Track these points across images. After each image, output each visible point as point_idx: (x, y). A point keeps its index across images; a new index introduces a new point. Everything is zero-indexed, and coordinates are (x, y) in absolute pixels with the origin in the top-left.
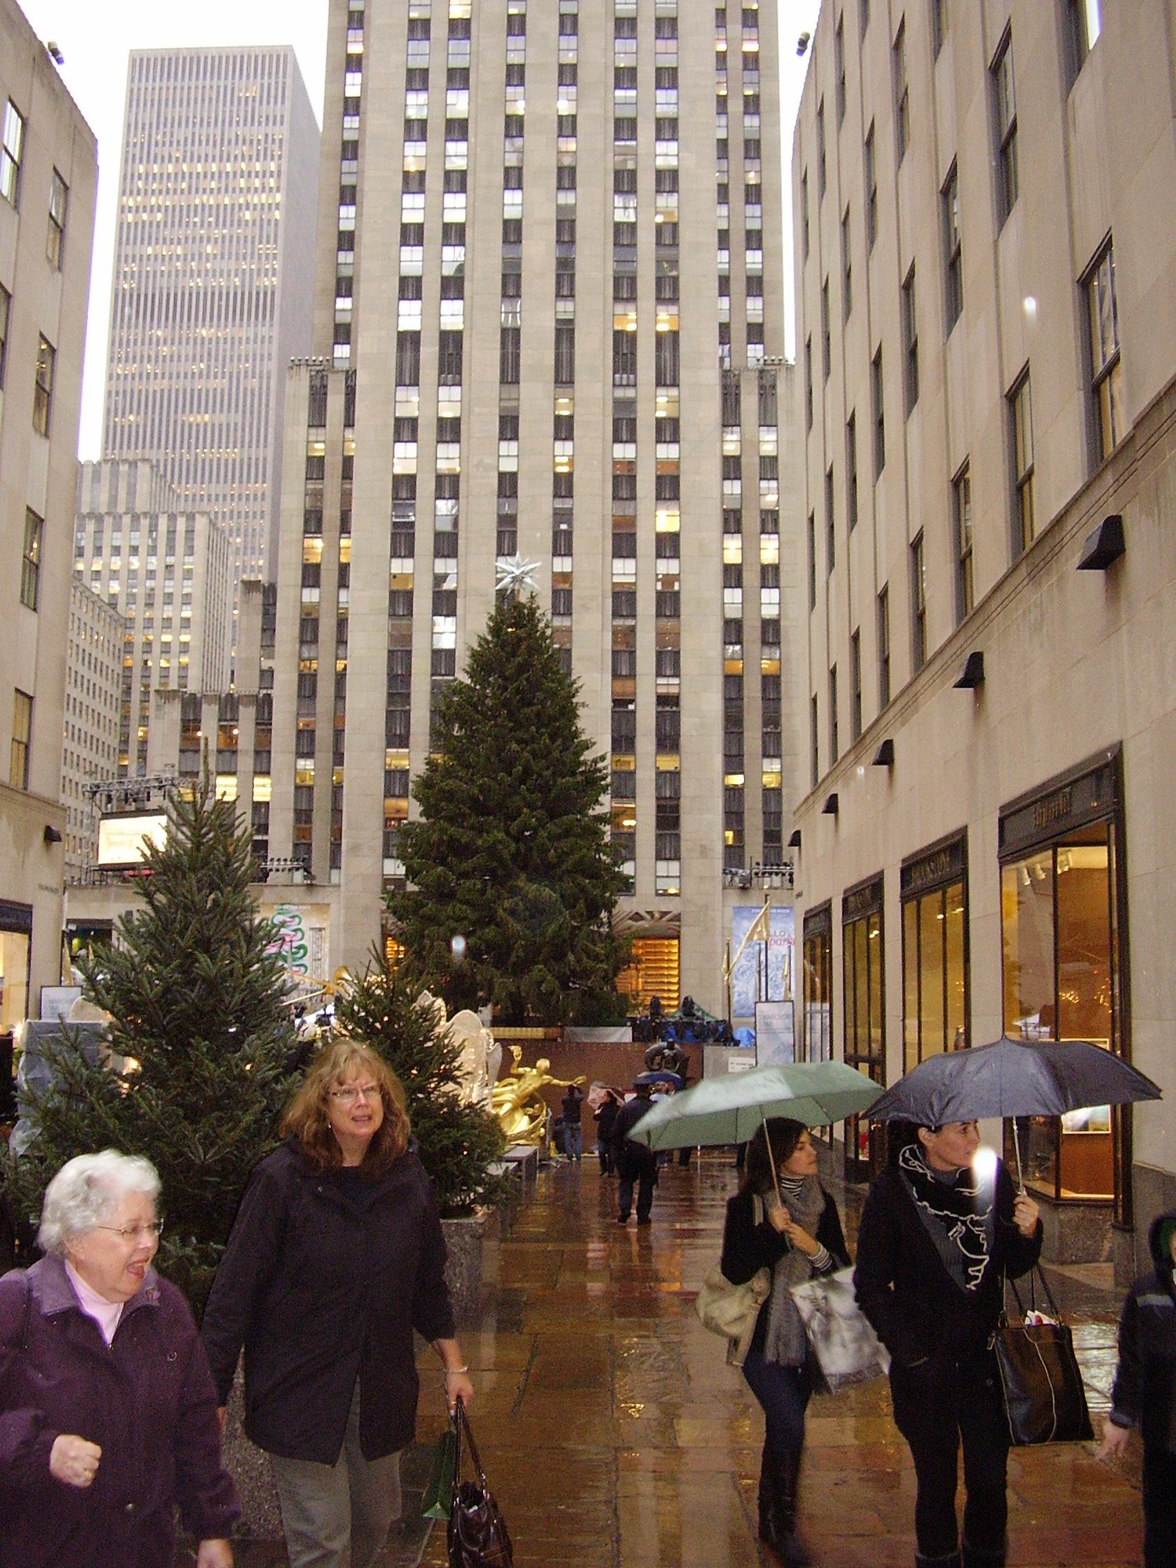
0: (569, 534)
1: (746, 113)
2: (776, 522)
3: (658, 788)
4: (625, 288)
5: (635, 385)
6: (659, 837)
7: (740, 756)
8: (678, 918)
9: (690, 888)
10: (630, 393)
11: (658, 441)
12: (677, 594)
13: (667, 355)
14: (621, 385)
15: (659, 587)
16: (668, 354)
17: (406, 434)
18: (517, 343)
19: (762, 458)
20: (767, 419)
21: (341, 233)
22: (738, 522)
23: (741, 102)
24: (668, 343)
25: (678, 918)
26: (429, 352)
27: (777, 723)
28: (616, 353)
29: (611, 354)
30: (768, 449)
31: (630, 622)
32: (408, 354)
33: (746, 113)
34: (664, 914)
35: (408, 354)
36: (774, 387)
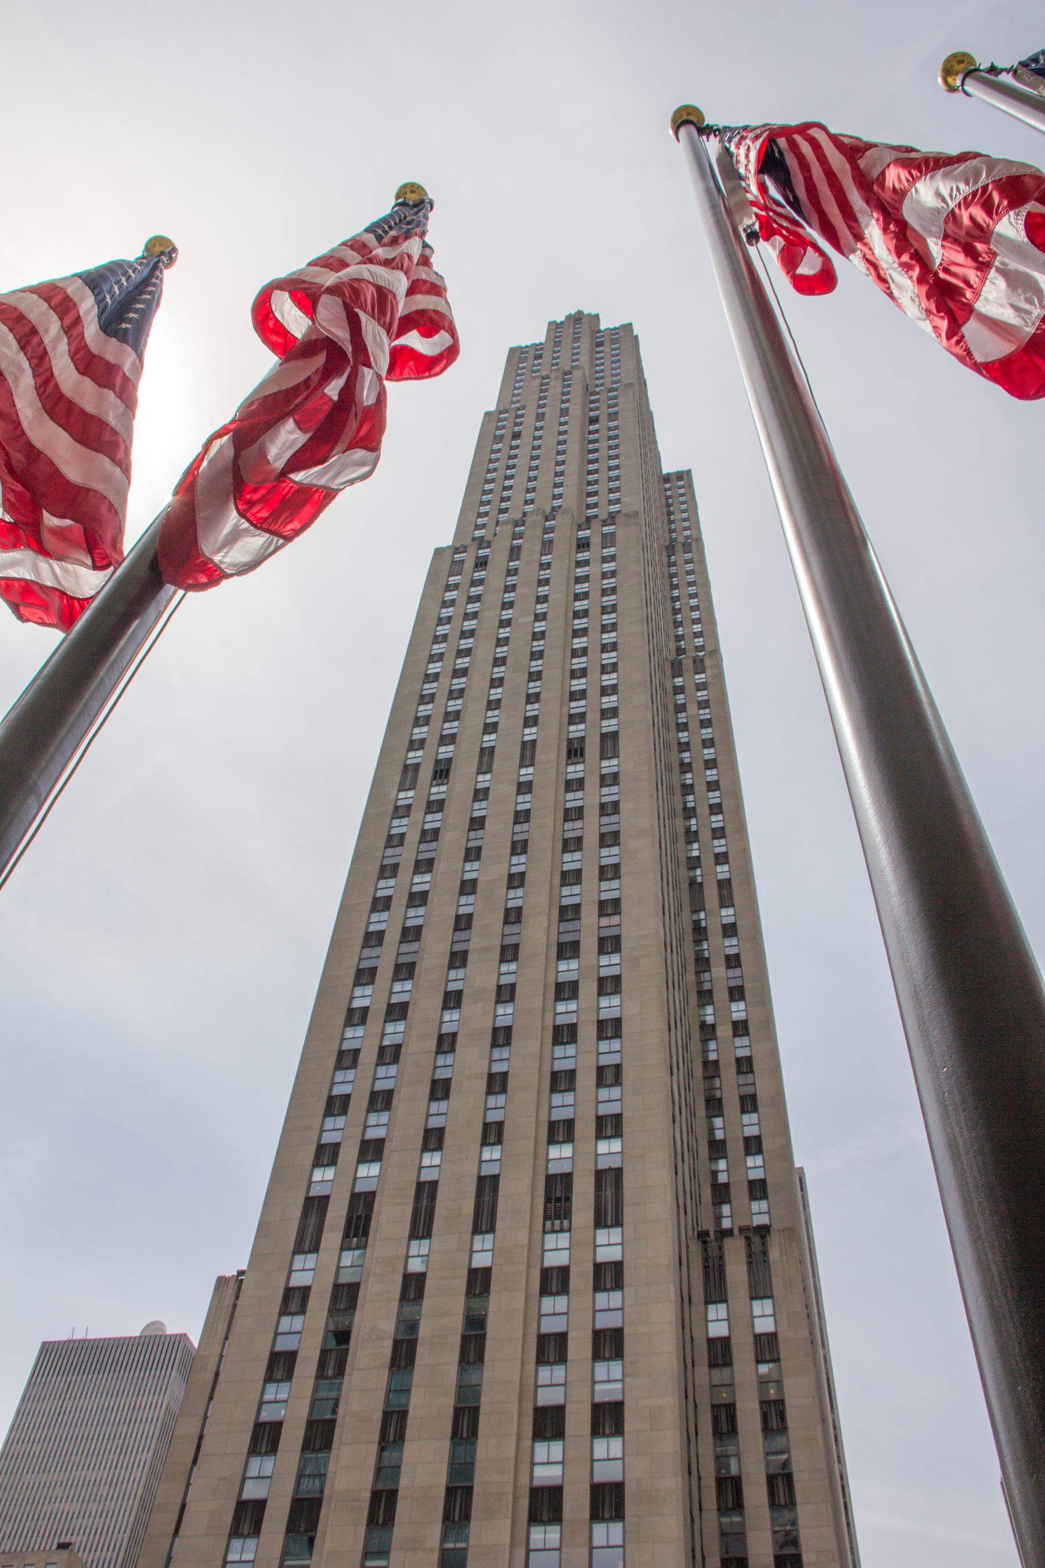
5: (570, 1230)
13: (609, 1193)
14: (553, 1231)
16: (609, 1193)
17: (294, 1306)
18: (433, 1197)
19: (757, 1337)
20: (760, 1290)
23: (730, 1027)
26: (337, 1214)
28: (548, 1200)
29: (540, 1200)
30: (764, 1326)
32: (313, 1220)
35: (313, 1220)
36: (765, 1253)
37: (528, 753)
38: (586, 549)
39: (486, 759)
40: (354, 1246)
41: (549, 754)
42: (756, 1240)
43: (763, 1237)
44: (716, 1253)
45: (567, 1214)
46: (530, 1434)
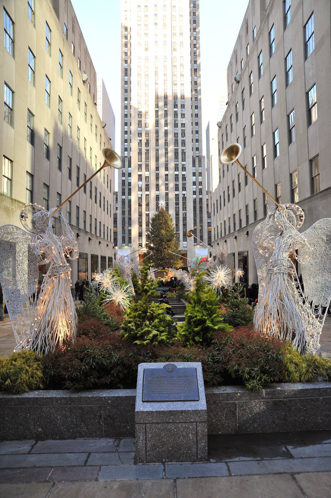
0: (168, 187)
1: (195, 109)
2: (201, 184)
3: (183, 230)
6: (183, 238)
7: (196, 223)
8: (187, 251)
9: (188, 246)
10: (177, 163)
11: (182, 171)
12: (186, 197)
15: (183, 196)
19: (199, 173)
21: (125, 131)
22: (195, 184)
24: (184, 153)
25: (187, 251)
27: (202, 218)
31: (178, 202)
32: (140, 156)
33: (195, 109)
34: (184, 250)
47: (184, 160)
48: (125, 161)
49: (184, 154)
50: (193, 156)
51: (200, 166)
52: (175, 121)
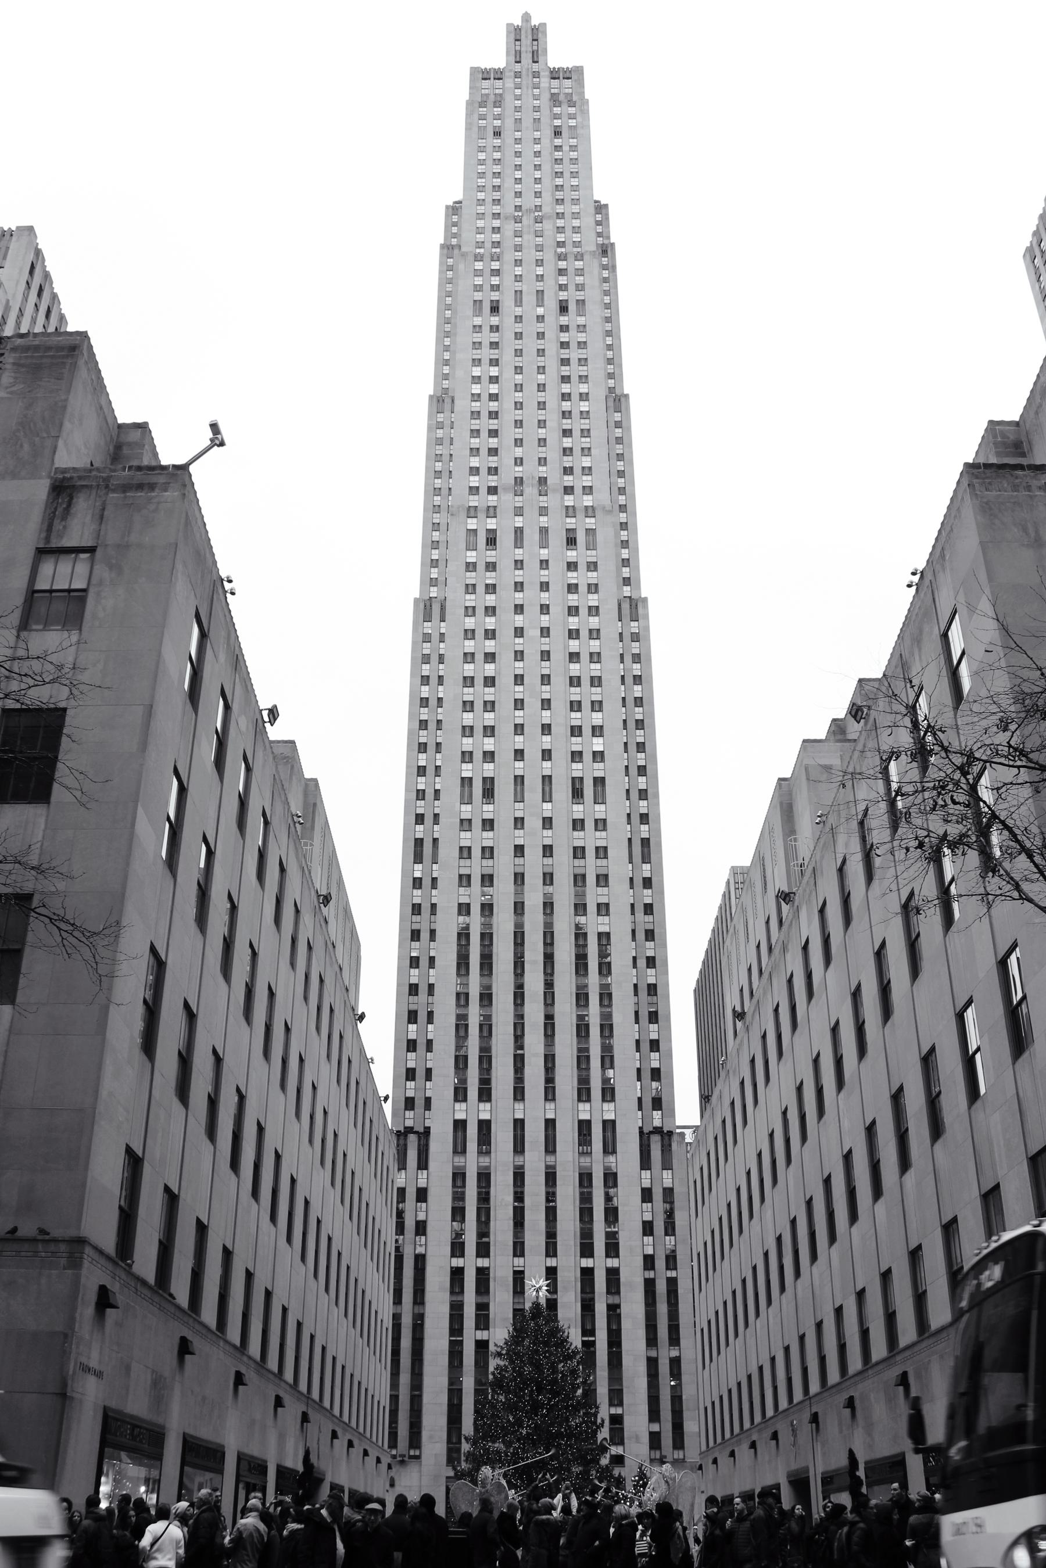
1: (648, 967)
4: (584, 1094)
13: (609, 1134)
14: (583, 1153)
17: (459, 1183)
20: (667, 1165)
23: (645, 961)
24: (609, 1126)
26: (472, 1131)
28: (580, 1135)
32: (460, 1134)
36: (670, 1145)
37: (547, 789)
38: (574, 547)
39: (519, 788)
40: (484, 1151)
41: (562, 790)
42: (666, 1138)
43: (670, 1136)
44: (646, 1143)
45: (590, 1144)
46: (579, 1255)
47: (610, 1148)
48: (405, 1145)
49: (609, 1127)
50: (641, 1128)
51: (667, 1165)
52: (581, 1018)
